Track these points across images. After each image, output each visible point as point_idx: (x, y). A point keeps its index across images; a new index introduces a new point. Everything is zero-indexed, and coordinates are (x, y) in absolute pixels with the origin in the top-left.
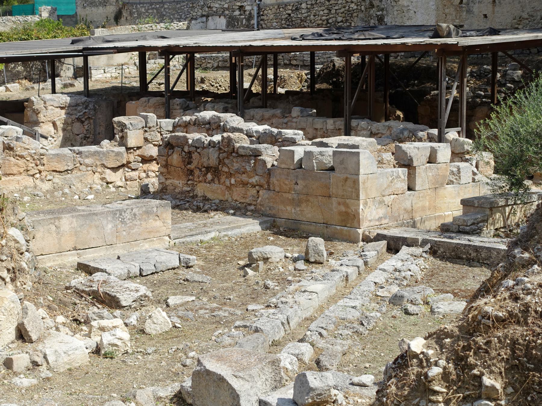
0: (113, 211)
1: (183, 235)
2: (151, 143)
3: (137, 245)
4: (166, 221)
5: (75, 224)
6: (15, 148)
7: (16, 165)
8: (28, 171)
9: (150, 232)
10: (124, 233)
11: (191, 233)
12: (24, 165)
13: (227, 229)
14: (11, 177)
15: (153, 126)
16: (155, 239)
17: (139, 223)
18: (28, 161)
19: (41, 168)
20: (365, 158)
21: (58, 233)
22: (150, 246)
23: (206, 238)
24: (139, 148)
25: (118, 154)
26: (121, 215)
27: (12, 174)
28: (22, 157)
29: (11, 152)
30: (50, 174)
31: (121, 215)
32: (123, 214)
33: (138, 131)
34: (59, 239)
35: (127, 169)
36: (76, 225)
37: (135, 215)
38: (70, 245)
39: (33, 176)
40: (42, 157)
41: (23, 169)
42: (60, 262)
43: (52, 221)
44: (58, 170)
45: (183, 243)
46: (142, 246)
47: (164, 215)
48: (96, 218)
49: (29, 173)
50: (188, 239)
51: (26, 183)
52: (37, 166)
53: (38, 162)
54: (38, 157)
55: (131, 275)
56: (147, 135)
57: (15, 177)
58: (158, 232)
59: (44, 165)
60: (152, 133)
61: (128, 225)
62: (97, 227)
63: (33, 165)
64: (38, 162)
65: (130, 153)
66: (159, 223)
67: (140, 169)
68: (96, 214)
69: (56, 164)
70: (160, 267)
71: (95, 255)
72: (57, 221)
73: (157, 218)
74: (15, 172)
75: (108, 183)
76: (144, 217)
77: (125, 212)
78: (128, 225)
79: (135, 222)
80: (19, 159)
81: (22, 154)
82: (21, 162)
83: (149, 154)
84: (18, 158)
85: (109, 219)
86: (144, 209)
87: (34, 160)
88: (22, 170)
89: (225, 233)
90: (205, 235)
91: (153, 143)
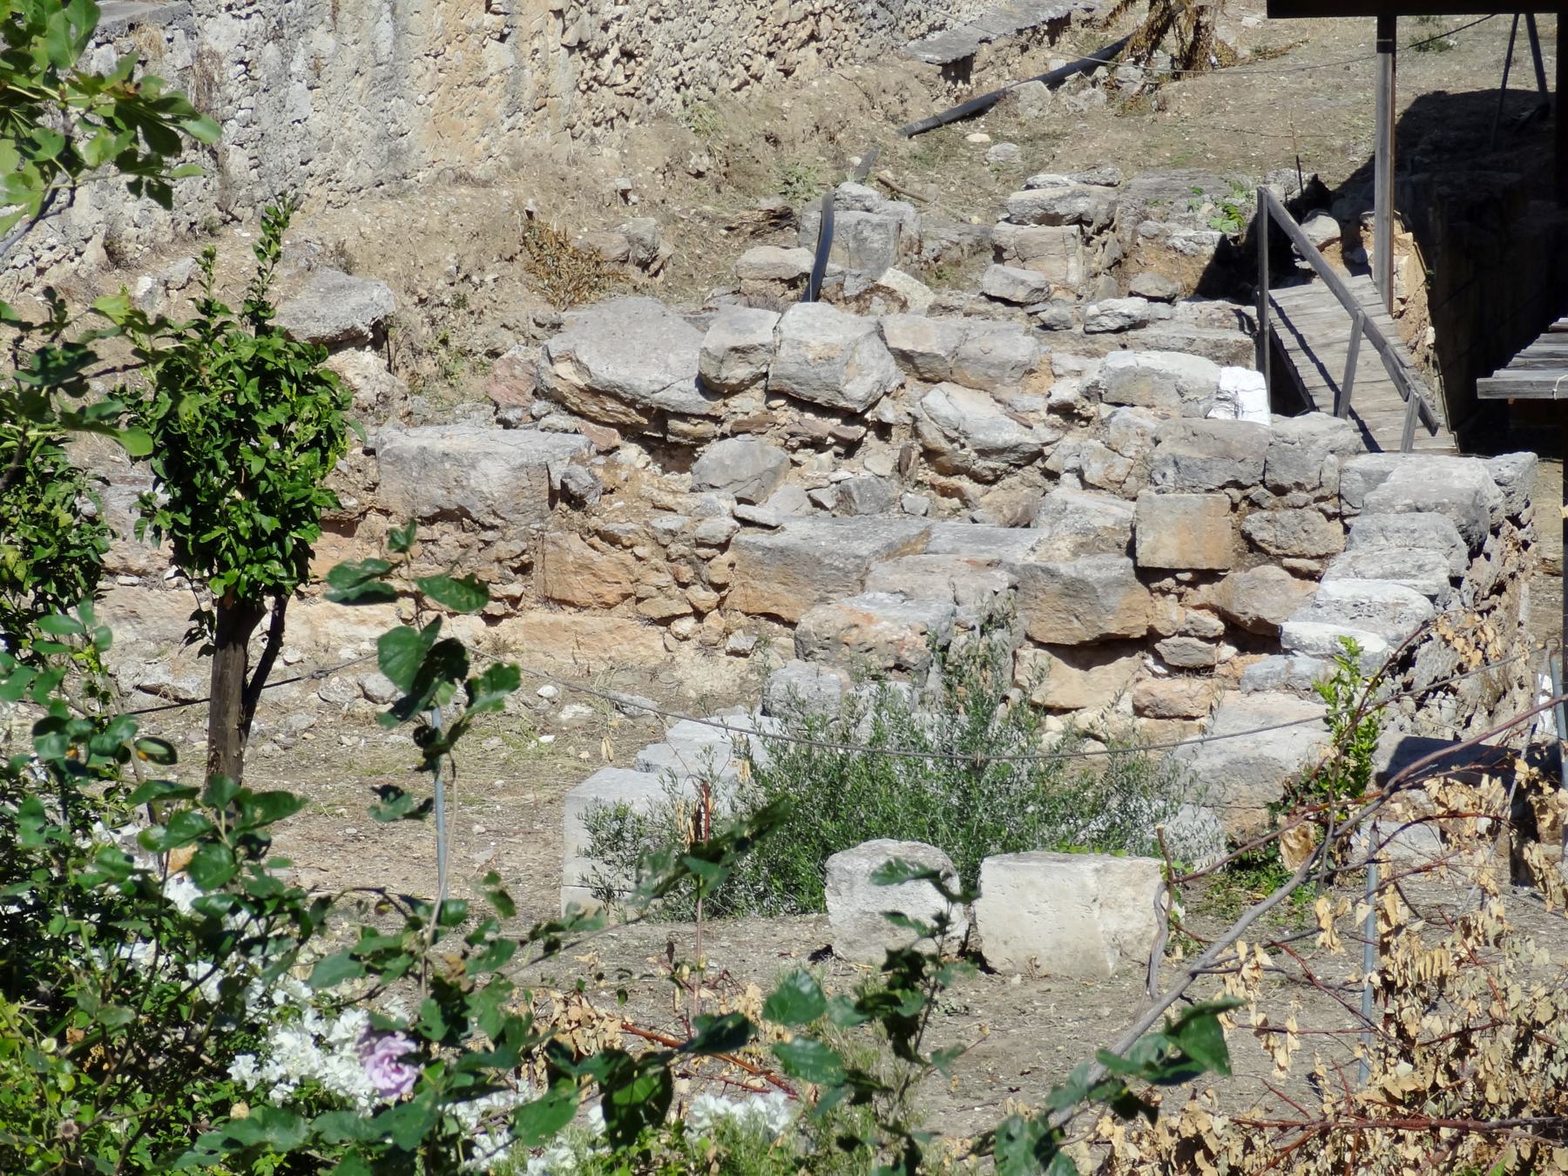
2: (1276, 559)
6: (592, 500)
7: (585, 567)
8: (639, 600)
12: (622, 575)
14: (565, 616)
15: (1299, 486)
18: (639, 559)
19: (703, 596)
24: (1209, 576)
25: (1075, 589)
27: (571, 604)
28: (613, 540)
29: (577, 516)
30: (748, 631)
33: (1196, 498)
35: (1150, 661)
39: (666, 621)
40: (703, 552)
41: (618, 590)
49: (649, 609)
51: (626, 647)
52: (684, 586)
53: (687, 573)
54: (683, 549)
56: (1254, 523)
57: (579, 617)
59: (719, 588)
60: (1287, 516)
63: (665, 579)
64: (687, 573)
65: (1165, 592)
67: (1220, 669)
69: (779, 588)
74: (580, 596)
75: (1050, 710)
80: (604, 546)
81: (612, 527)
82: (606, 559)
83: (1252, 613)
84: (596, 540)
87: (668, 558)
88: (611, 594)
91: (1287, 562)
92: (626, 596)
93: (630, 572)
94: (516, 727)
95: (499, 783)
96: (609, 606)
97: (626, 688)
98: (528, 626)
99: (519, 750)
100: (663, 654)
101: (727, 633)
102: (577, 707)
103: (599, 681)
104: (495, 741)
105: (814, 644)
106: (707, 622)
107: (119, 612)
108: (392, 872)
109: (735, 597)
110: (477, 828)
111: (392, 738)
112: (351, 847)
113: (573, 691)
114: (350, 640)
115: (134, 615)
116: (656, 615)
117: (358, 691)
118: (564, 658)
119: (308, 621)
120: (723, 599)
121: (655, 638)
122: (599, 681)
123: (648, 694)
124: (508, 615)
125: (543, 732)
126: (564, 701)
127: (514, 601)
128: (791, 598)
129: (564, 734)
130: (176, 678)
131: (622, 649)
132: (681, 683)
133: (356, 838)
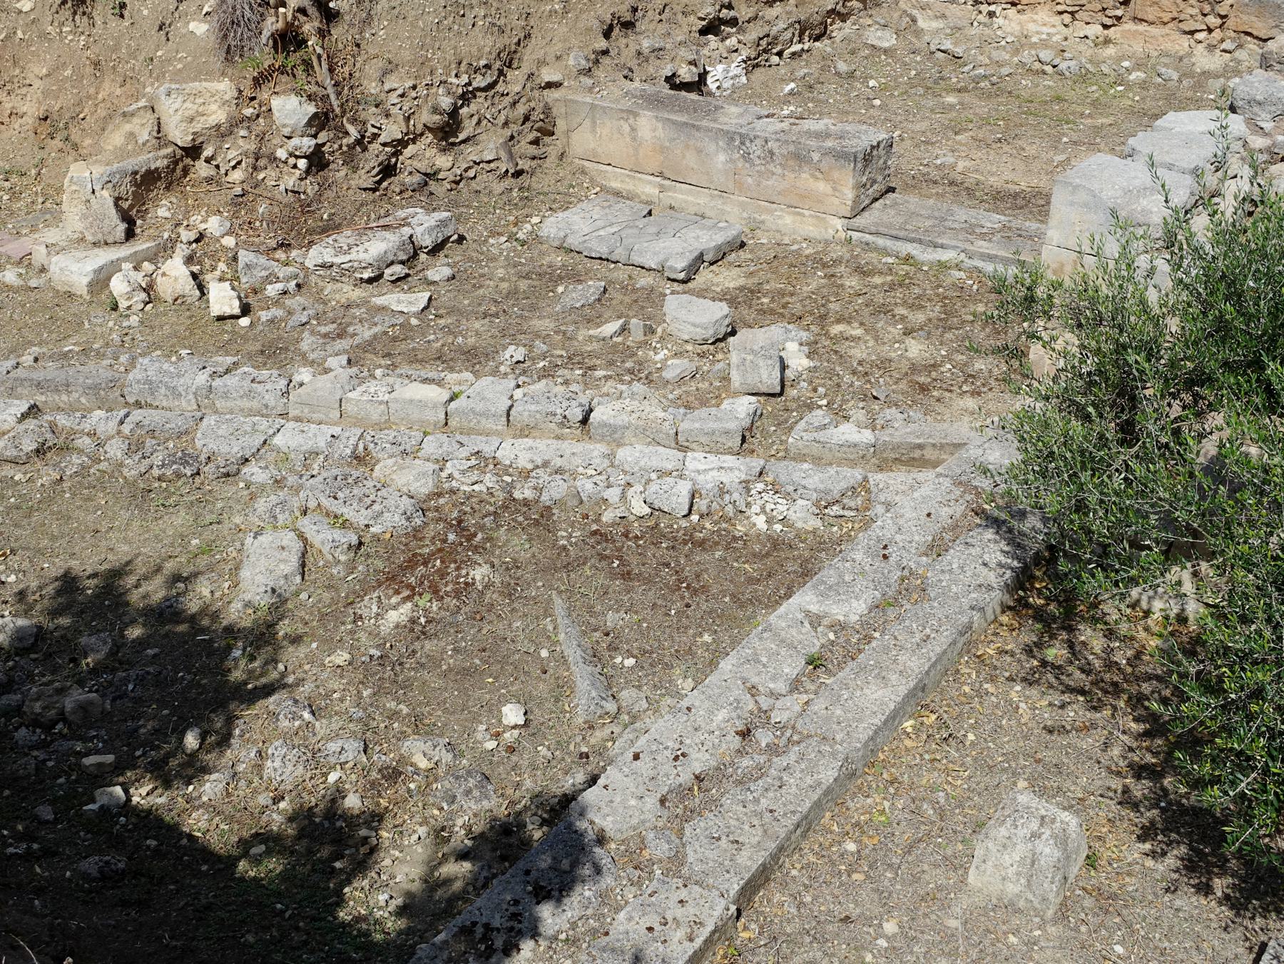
0: (728, 132)
1: (873, 229)
3: (771, 212)
4: (839, 187)
5: (660, 132)
8: (1181, 21)
9: (803, 197)
10: (750, 180)
11: (894, 233)
12: (1173, 8)
13: (990, 258)
14: (1142, 27)
16: (807, 213)
17: (779, 170)
19: (1213, 21)
20: (1072, 204)
21: (634, 139)
22: (794, 222)
23: (927, 256)
26: (743, 143)
27: (1146, 21)
30: (1233, 40)
31: (743, 143)
32: (748, 144)
34: (636, 150)
36: (662, 135)
37: (772, 153)
38: (653, 166)
39: (1192, 33)
41: (1170, 15)
42: (631, 187)
43: (625, 115)
44: (1255, 33)
45: (867, 244)
46: (780, 217)
47: (836, 175)
48: (698, 134)
50: (881, 242)
55: (565, 245)
57: (1149, 28)
58: (819, 201)
61: (757, 168)
62: (699, 151)
63: (1195, 11)
66: (822, 187)
68: (698, 128)
69: (1254, 19)
70: (619, 254)
71: (690, 198)
72: (631, 117)
73: (820, 176)
74: (1150, 18)
76: (791, 163)
77: (751, 141)
78: (757, 168)
79: (771, 167)
85: (721, 143)
86: (792, 148)
88: (1166, 17)
89: (980, 264)
90: (930, 250)
92: (1174, 19)
93: (1178, 7)
94: (1107, 81)
95: (1088, 112)
96: (1165, 24)
97: (1166, 65)
98: (1123, 31)
99: (1105, 92)
100: (1187, 49)
101: (1222, 41)
102: (1139, 74)
103: (1153, 61)
104: (1094, 88)
105: (1274, 60)
106: (1213, 34)
107: (938, 14)
108: (1008, 165)
109: (1230, 23)
110: (1065, 139)
111: (1046, 83)
112: (994, 146)
113: (1138, 66)
114: (1037, 33)
115: (944, 16)
116: (1187, 29)
117: (1036, 58)
118: (1138, 48)
119: (1020, 23)
120: (1224, 23)
121: (1185, 41)
122: (1153, 61)
123: (1176, 69)
124: (1114, 25)
125: (1120, 85)
126: (1133, 70)
127: (1119, 18)
128: (1260, 25)
129: (1129, 87)
130: (955, 47)
131: (1167, 46)
132: (1194, 64)
133: (999, 140)
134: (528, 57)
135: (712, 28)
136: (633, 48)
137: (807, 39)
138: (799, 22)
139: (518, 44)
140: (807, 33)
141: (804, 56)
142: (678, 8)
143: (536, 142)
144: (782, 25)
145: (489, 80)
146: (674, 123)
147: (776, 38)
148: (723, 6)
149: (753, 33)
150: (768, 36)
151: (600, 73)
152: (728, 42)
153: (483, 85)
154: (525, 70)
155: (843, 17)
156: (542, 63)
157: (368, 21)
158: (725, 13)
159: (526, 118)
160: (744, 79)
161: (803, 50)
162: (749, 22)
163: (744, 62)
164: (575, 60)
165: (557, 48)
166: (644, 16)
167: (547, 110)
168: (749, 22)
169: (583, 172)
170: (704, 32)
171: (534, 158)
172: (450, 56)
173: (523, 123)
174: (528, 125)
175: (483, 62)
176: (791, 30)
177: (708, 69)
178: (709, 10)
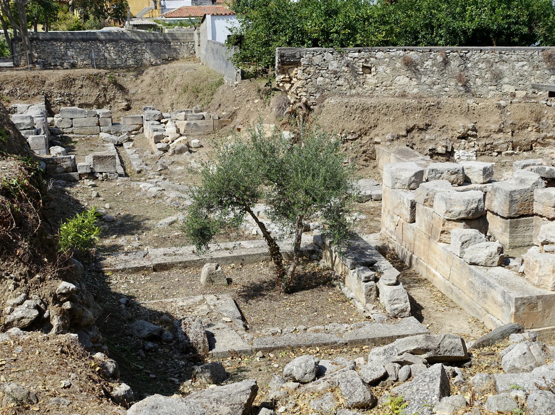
134: (373, 133)
135: (464, 137)
136: (421, 137)
137: (518, 150)
138: (512, 142)
139: (371, 128)
140: (518, 147)
141: (513, 156)
142: (451, 128)
143: (366, 160)
144: (501, 141)
145: (354, 137)
146: (397, 158)
147: (496, 146)
148: (469, 130)
149: (483, 142)
150: (492, 144)
151: (396, 142)
152: (471, 143)
153: (351, 138)
154: (370, 137)
155: (544, 145)
156: (377, 135)
157: (320, 113)
158: (470, 132)
159: (364, 152)
160: (474, 158)
161: (512, 154)
162: (484, 137)
163: (476, 151)
164: (389, 136)
165: (384, 131)
166: (433, 128)
167: (374, 151)
168: (484, 137)
169: (379, 174)
170: (458, 138)
171: (363, 165)
172: (340, 127)
173: (363, 153)
174: (365, 154)
175: (352, 131)
176: (507, 144)
177: (455, 150)
178: (462, 130)
